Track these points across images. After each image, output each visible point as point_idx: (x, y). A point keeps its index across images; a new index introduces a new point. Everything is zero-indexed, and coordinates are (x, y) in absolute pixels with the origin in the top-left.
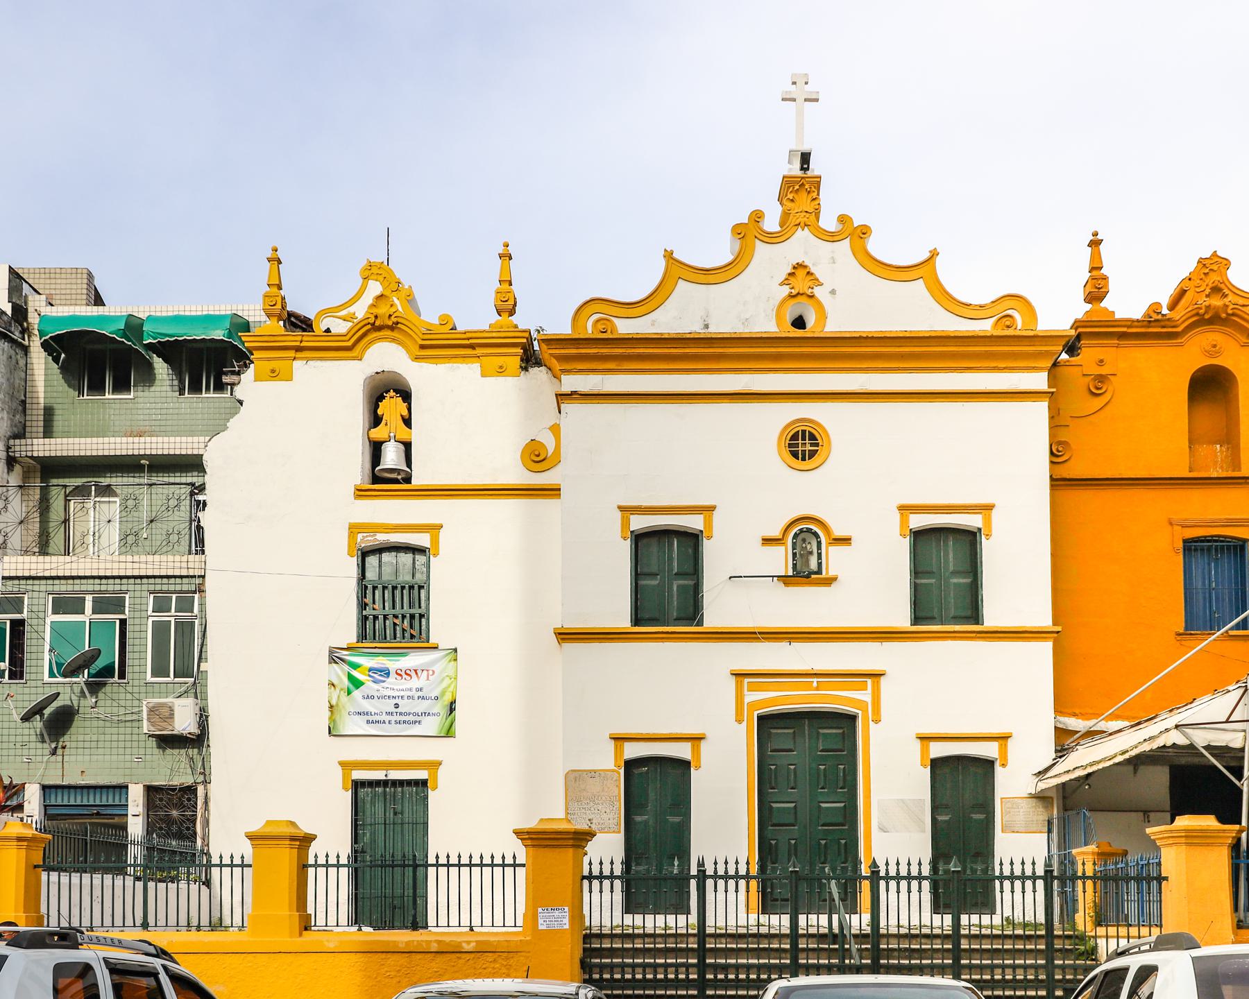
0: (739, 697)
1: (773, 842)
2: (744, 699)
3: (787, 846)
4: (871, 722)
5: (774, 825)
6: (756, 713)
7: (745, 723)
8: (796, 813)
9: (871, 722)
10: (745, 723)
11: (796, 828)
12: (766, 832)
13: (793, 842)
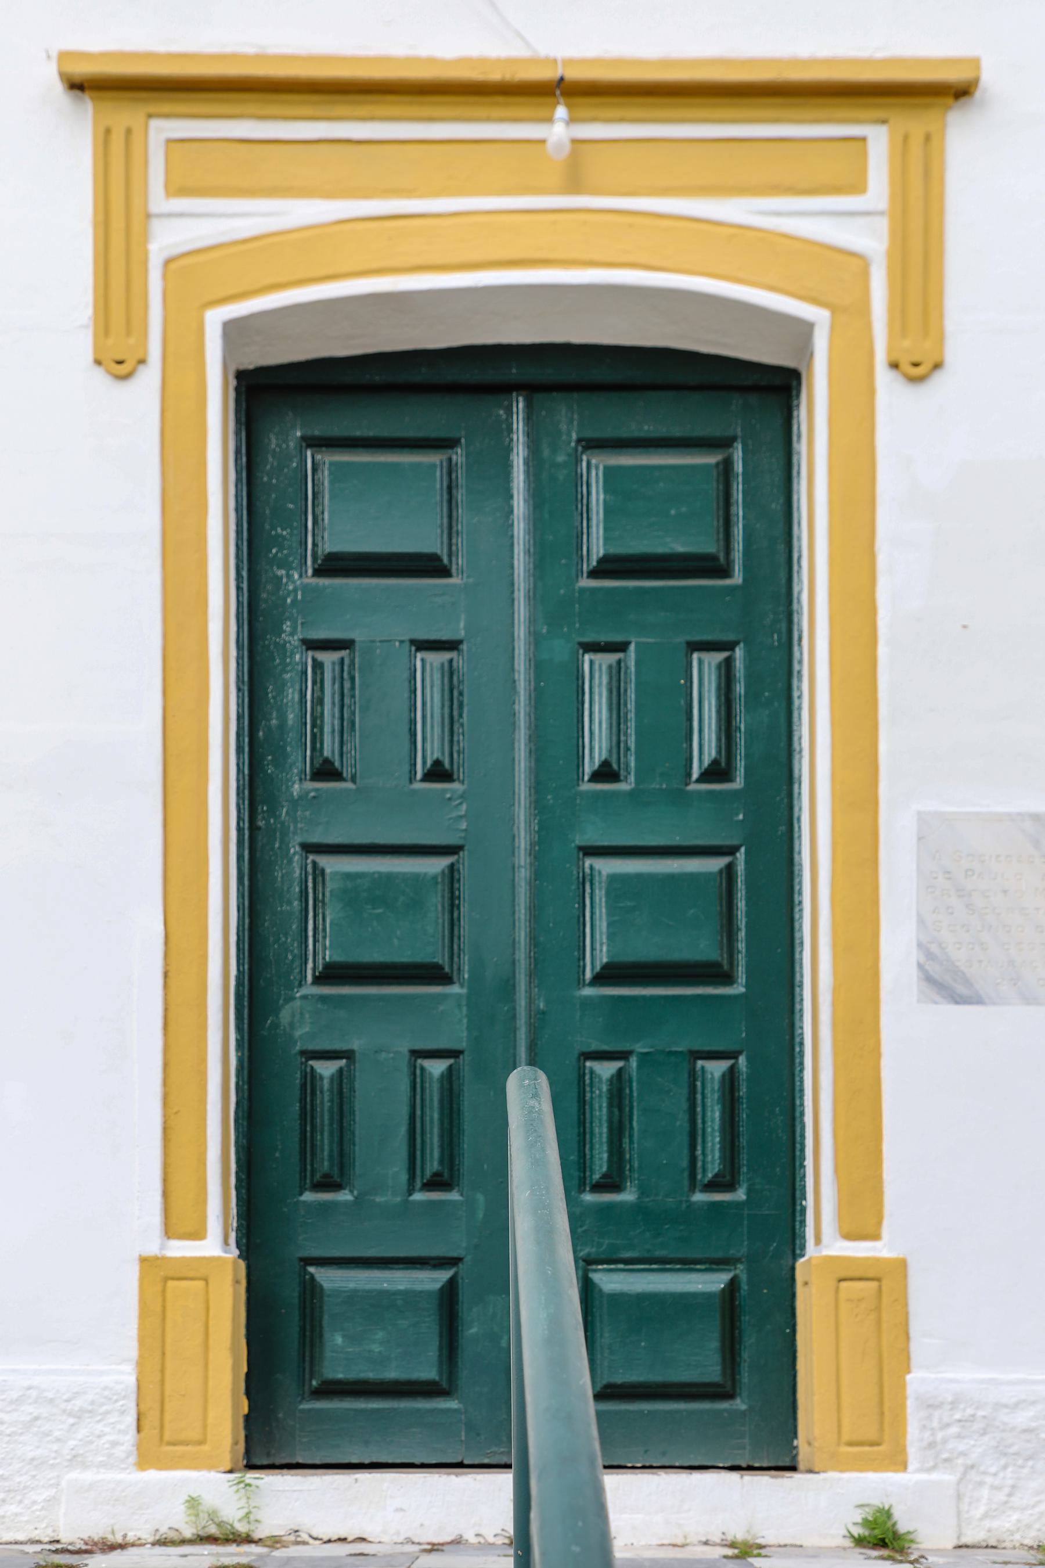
0: (118, 224)
1: (326, 1069)
2: (146, 236)
3: (404, 1086)
4: (883, 376)
5: (331, 975)
6: (215, 319)
7: (150, 377)
8: (453, 903)
9: (883, 376)
10: (150, 377)
11: (455, 989)
12: (285, 1015)
13: (437, 1068)
